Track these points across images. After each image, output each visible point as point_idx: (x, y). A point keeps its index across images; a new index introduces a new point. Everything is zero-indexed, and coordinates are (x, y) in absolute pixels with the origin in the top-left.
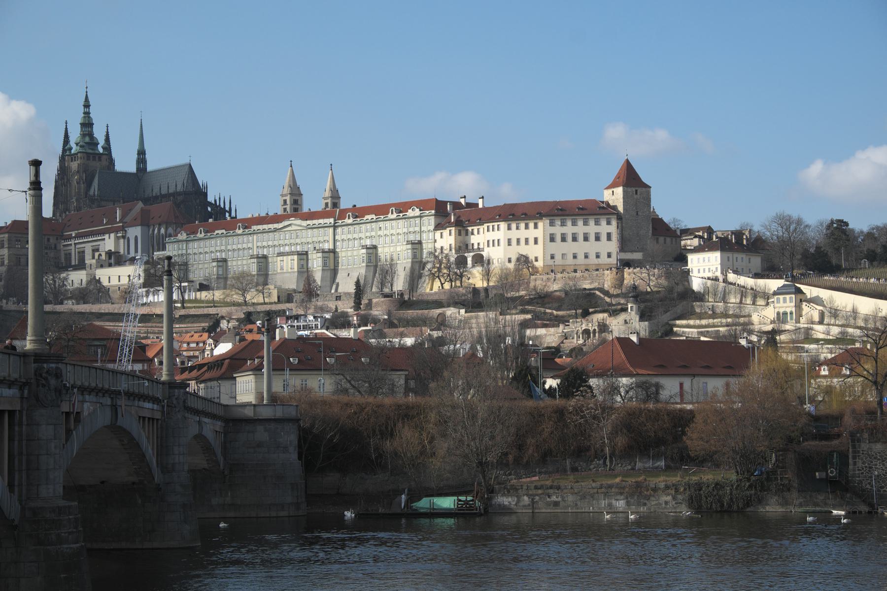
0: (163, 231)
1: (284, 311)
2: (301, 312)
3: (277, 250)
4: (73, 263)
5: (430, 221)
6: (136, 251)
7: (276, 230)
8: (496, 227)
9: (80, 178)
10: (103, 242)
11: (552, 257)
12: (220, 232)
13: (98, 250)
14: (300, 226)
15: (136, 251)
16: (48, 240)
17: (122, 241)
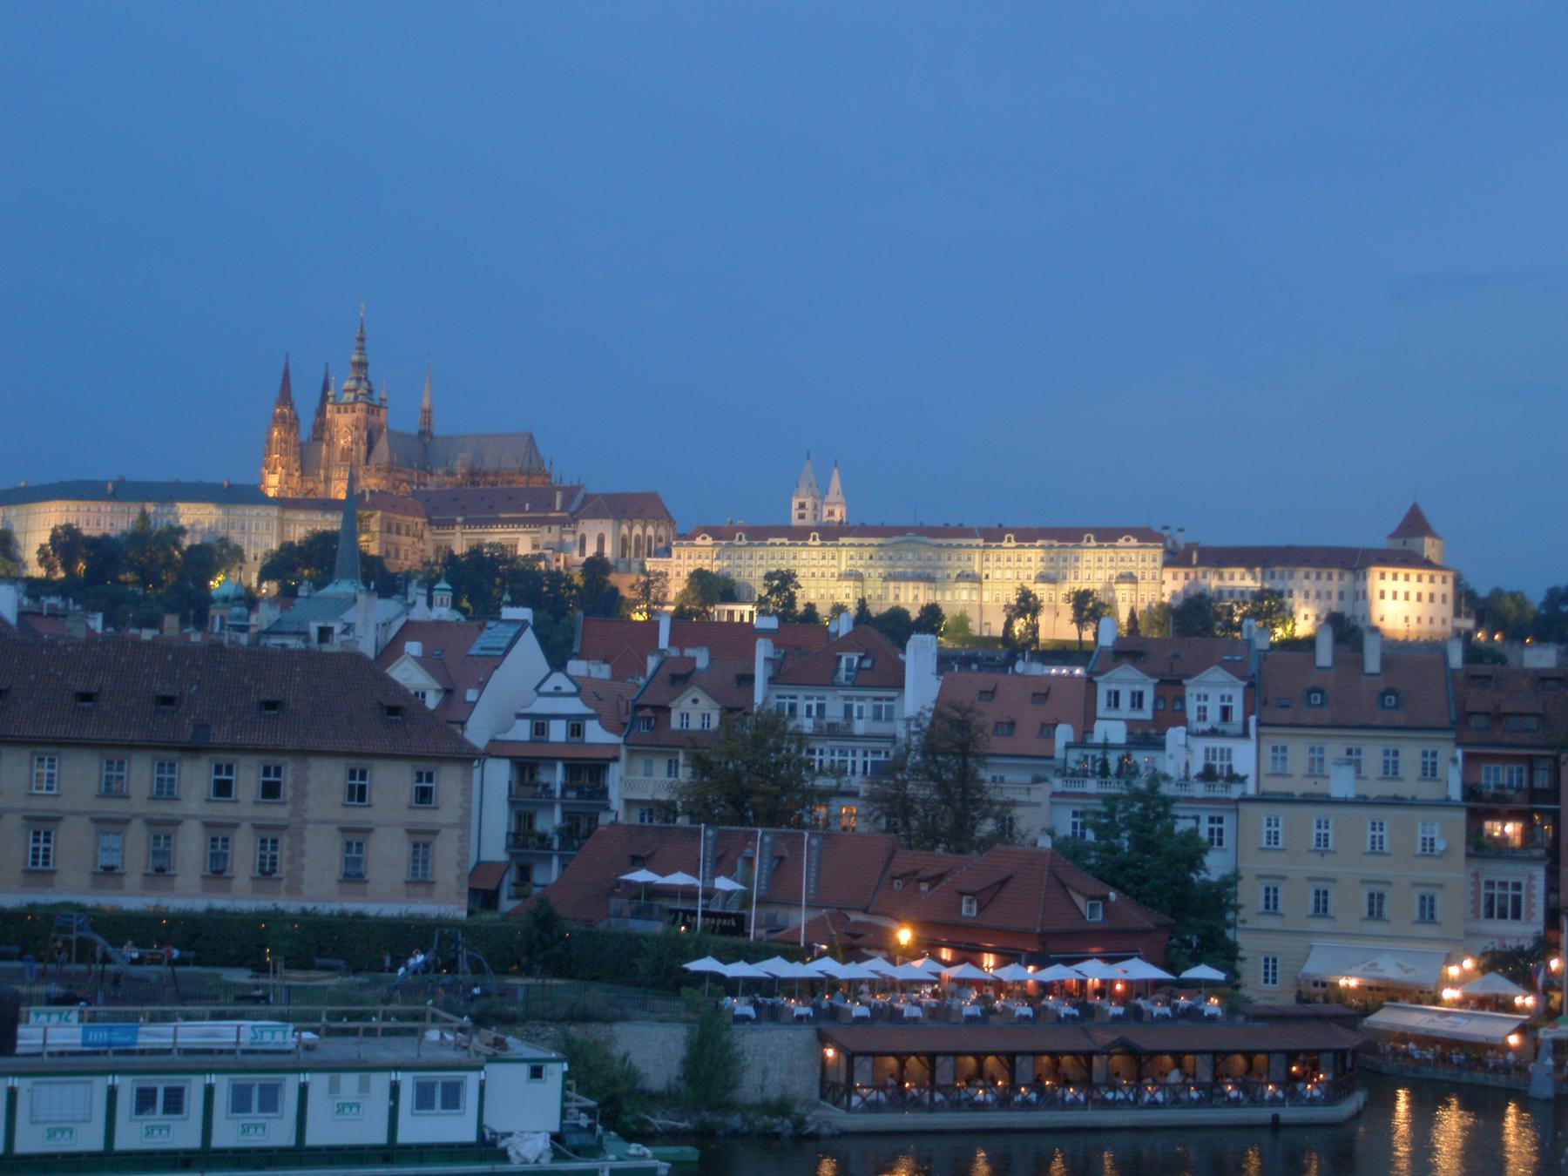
0: (650, 531)
9: (360, 437)
11: (1382, 619)
12: (778, 541)
13: (516, 546)
16: (417, 524)
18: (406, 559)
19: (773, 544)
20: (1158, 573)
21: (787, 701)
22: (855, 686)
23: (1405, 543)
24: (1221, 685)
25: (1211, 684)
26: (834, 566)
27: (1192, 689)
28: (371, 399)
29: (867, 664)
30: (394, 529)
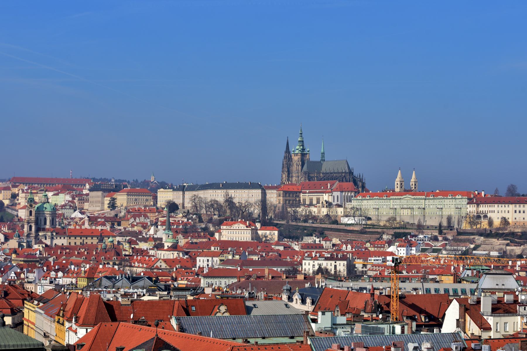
0: (349, 194)
1: (411, 233)
2: (417, 234)
3: (402, 207)
4: (307, 203)
5: (465, 201)
6: (338, 201)
7: (400, 199)
8: (493, 206)
9: (299, 163)
10: (323, 196)
11: (515, 219)
12: (376, 197)
13: (319, 199)
15: (338, 201)
17: (330, 197)
19: (375, 199)
26: (389, 205)
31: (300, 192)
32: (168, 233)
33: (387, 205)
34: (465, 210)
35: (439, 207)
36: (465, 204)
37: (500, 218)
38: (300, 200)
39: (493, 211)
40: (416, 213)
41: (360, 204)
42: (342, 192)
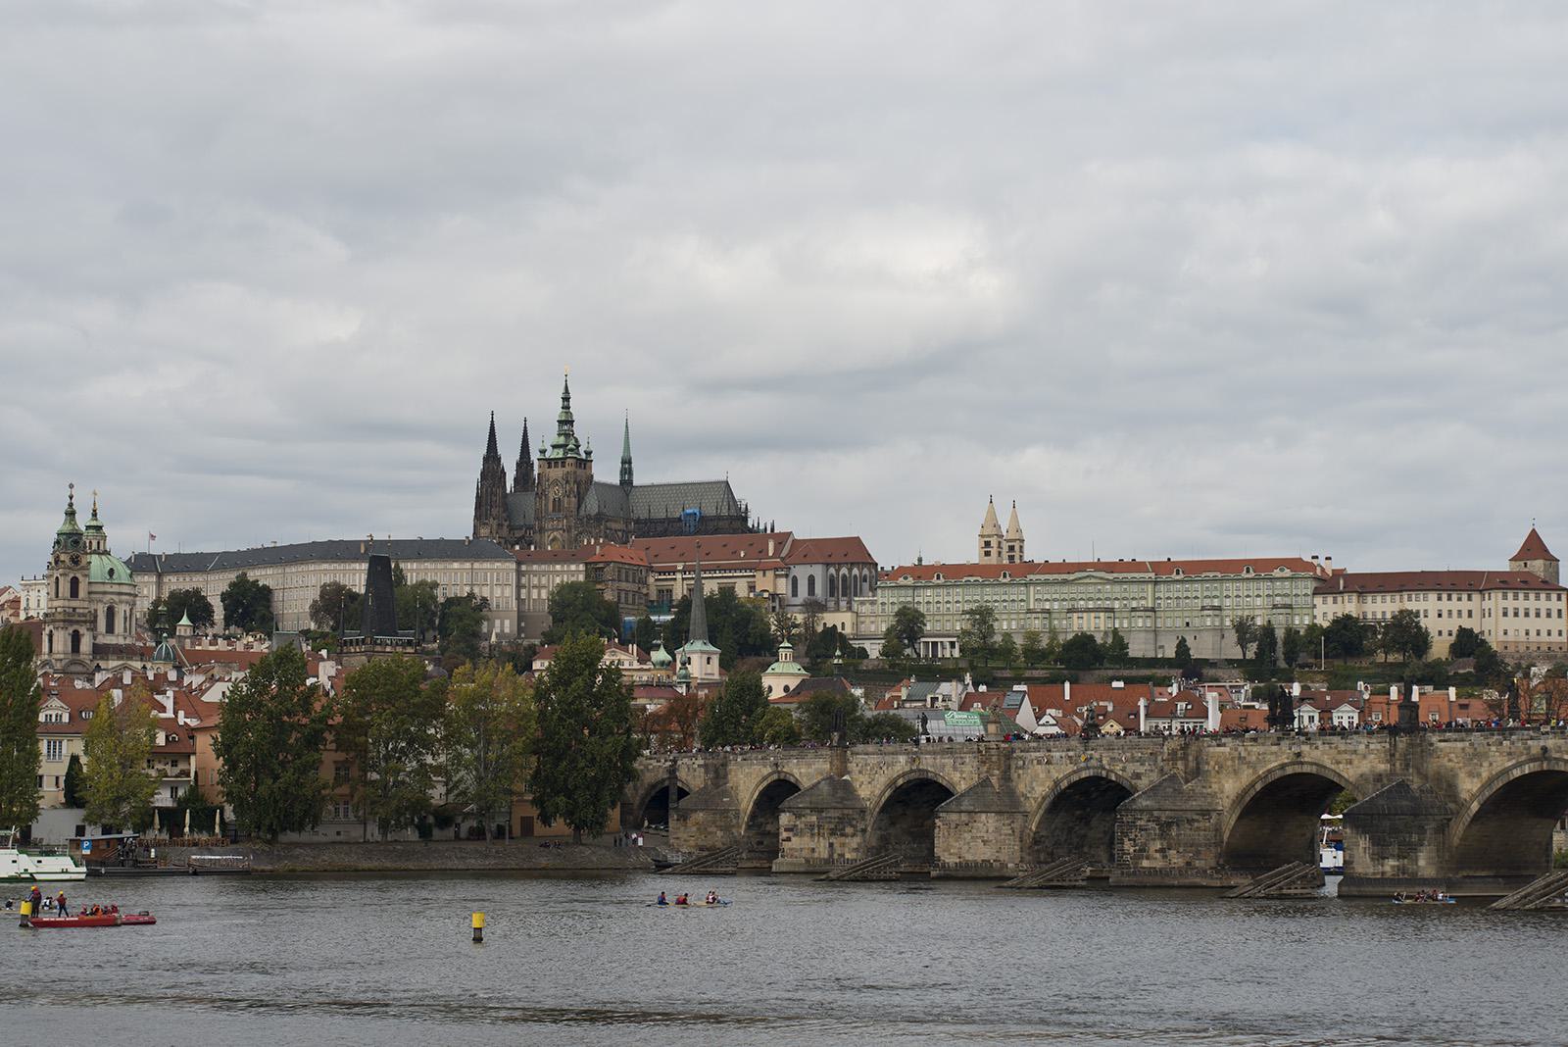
0: (855, 571)
9: (571, 489)
10: (752, 580)
11: (1505, 633)
12: (972, 579)
13: (734, 588)
14: (1101, 578)
17: (783, 580)
18: (633, 603)
20: (1309, 599)
21: (1154, 725)
22: (1185, 717)
23: (1525, 564)
24: (1348, 712)
25: (1343, 712)
26: (1022, 601)
27: (1335, 715)
28: (580, 455)
29: (1189, 707)
30: (623, 577)
31: (651, 569)
32: (705, 648)
33: (1013, 601)
34: (1305, 611)
35: (1207, 602)
36: (1306, 595)
37: (1445, 633)
38: (647, 595)
39: (1422, 614)
40: (1121, 623)
41: (910, 599)
42: (828, 565)
